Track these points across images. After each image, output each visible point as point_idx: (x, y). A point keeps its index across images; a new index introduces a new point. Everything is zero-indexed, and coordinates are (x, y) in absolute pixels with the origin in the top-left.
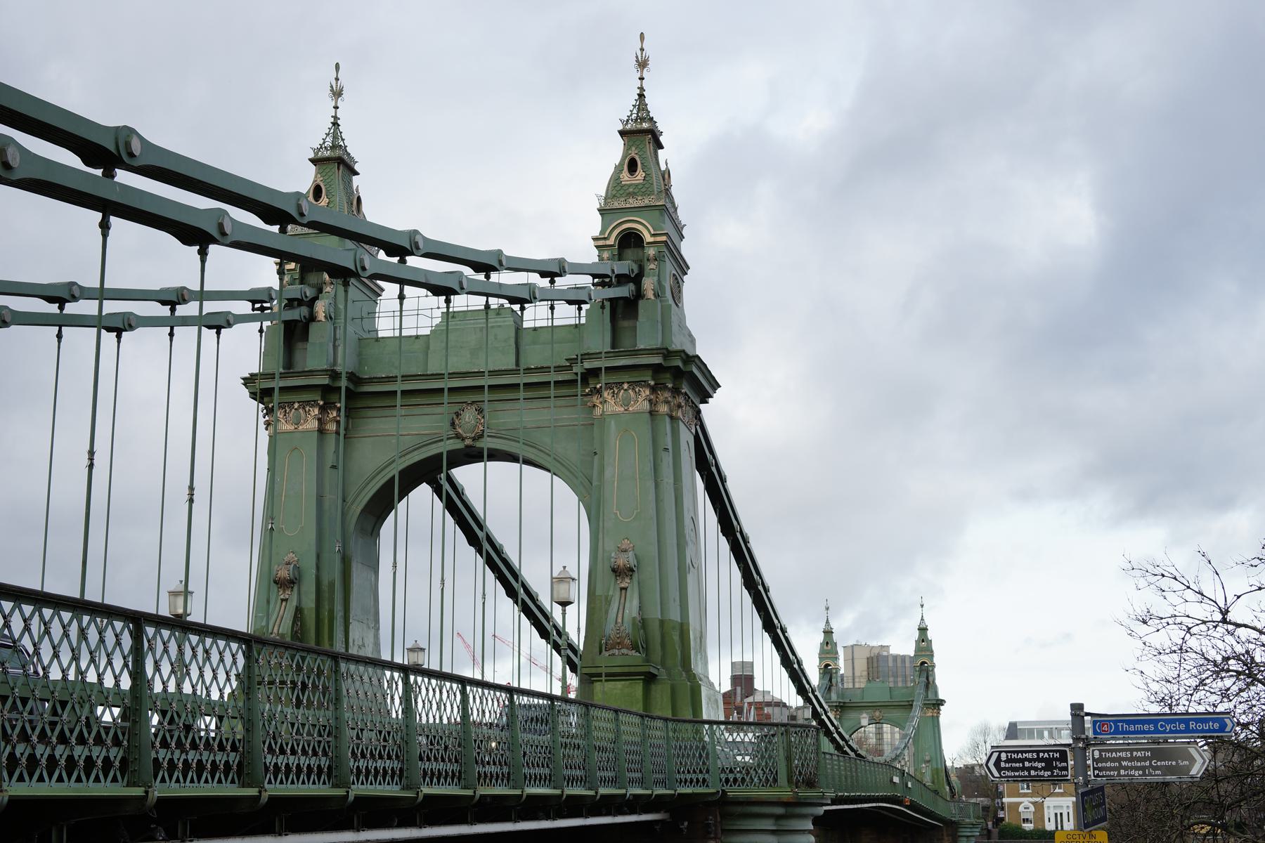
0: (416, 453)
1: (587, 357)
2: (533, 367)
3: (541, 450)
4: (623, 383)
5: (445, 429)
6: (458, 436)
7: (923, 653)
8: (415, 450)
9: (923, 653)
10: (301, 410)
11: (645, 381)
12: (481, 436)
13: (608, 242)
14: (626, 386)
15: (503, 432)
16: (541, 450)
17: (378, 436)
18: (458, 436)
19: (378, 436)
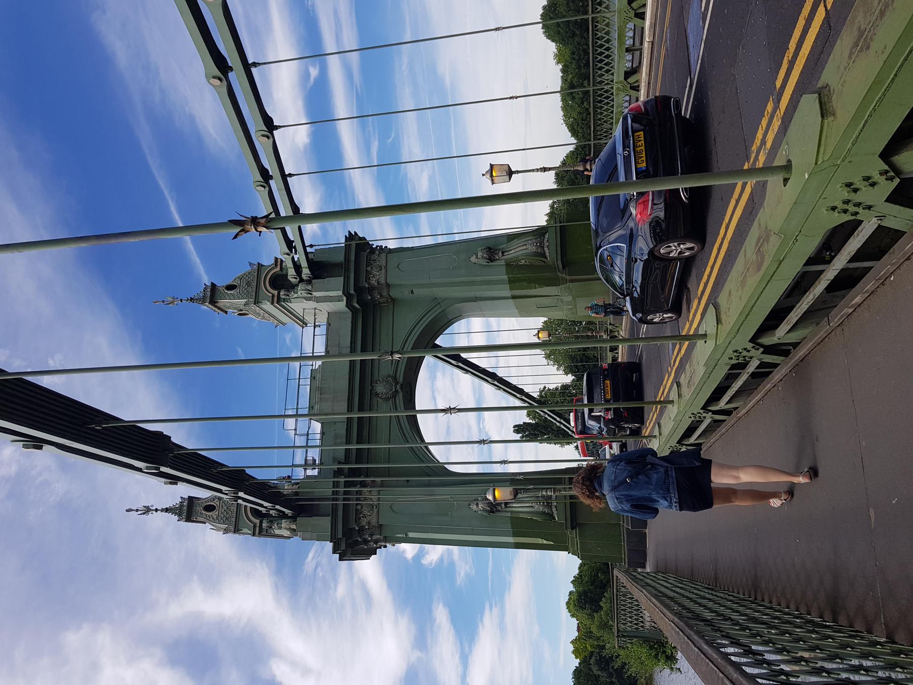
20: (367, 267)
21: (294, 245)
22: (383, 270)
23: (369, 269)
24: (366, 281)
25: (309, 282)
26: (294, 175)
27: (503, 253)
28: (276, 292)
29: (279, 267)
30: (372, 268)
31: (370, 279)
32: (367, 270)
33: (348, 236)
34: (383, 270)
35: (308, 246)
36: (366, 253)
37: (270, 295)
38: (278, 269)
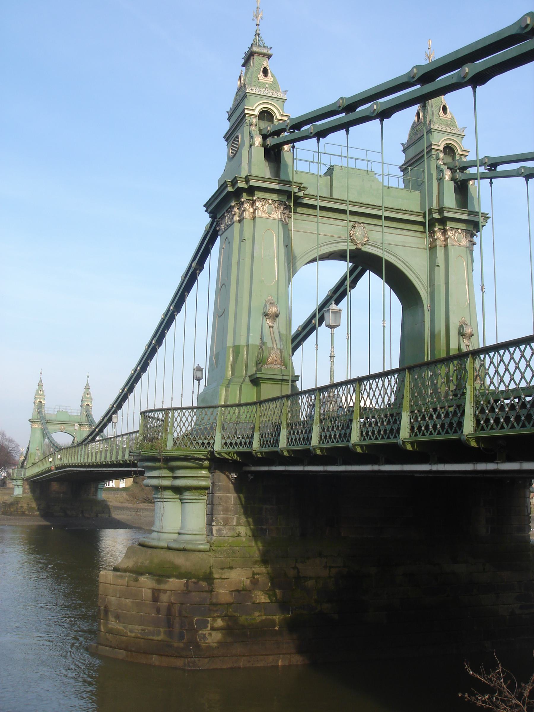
0: (326, 247)
1: (447, 210)
2: (403, 209)
3: (399, 259)
4: (458, 229)
5: (345, 236)
6: (353, 242)
7: (88, 400)
8: (327, 245)
9: (88, 400)
10: (272, 205)
11: (469, 230)
12: (366, 244)
13: (439, 148)
14: (459, 230)
15: (378, 244)
16: (399, 259)
17: (303, 232)
18: (353, 242)
19: (303, 232)
20: (272, 200)
21: (296, 131)
22: (267, 216)
23: (270, 202)
24: (259, 198)
25: (264, 145)
26: (347, 134)
27: (272, 327)
28: (256, 112)
29: (280, 118)
30: (271, 204)
31: (261, 202)
32: (269, 199)
33: (303, 185)
34: (267, 216)
35: (294, 144)
36: (285, 200)
37: (254, 109)
38: (279, 117)
